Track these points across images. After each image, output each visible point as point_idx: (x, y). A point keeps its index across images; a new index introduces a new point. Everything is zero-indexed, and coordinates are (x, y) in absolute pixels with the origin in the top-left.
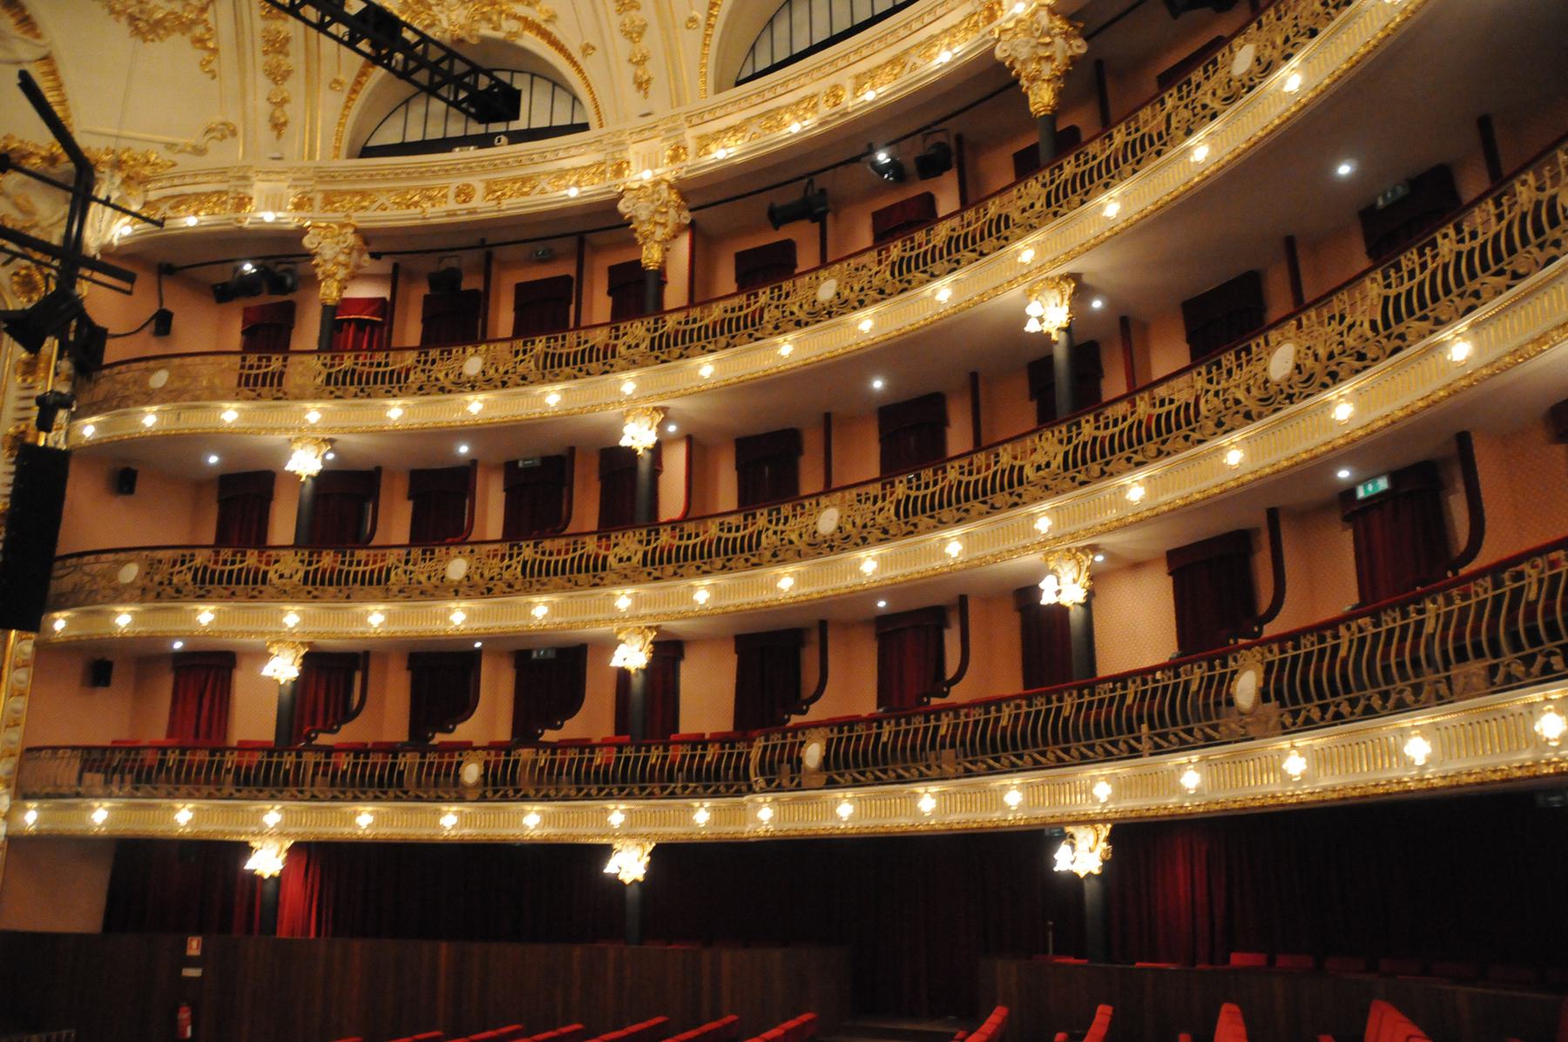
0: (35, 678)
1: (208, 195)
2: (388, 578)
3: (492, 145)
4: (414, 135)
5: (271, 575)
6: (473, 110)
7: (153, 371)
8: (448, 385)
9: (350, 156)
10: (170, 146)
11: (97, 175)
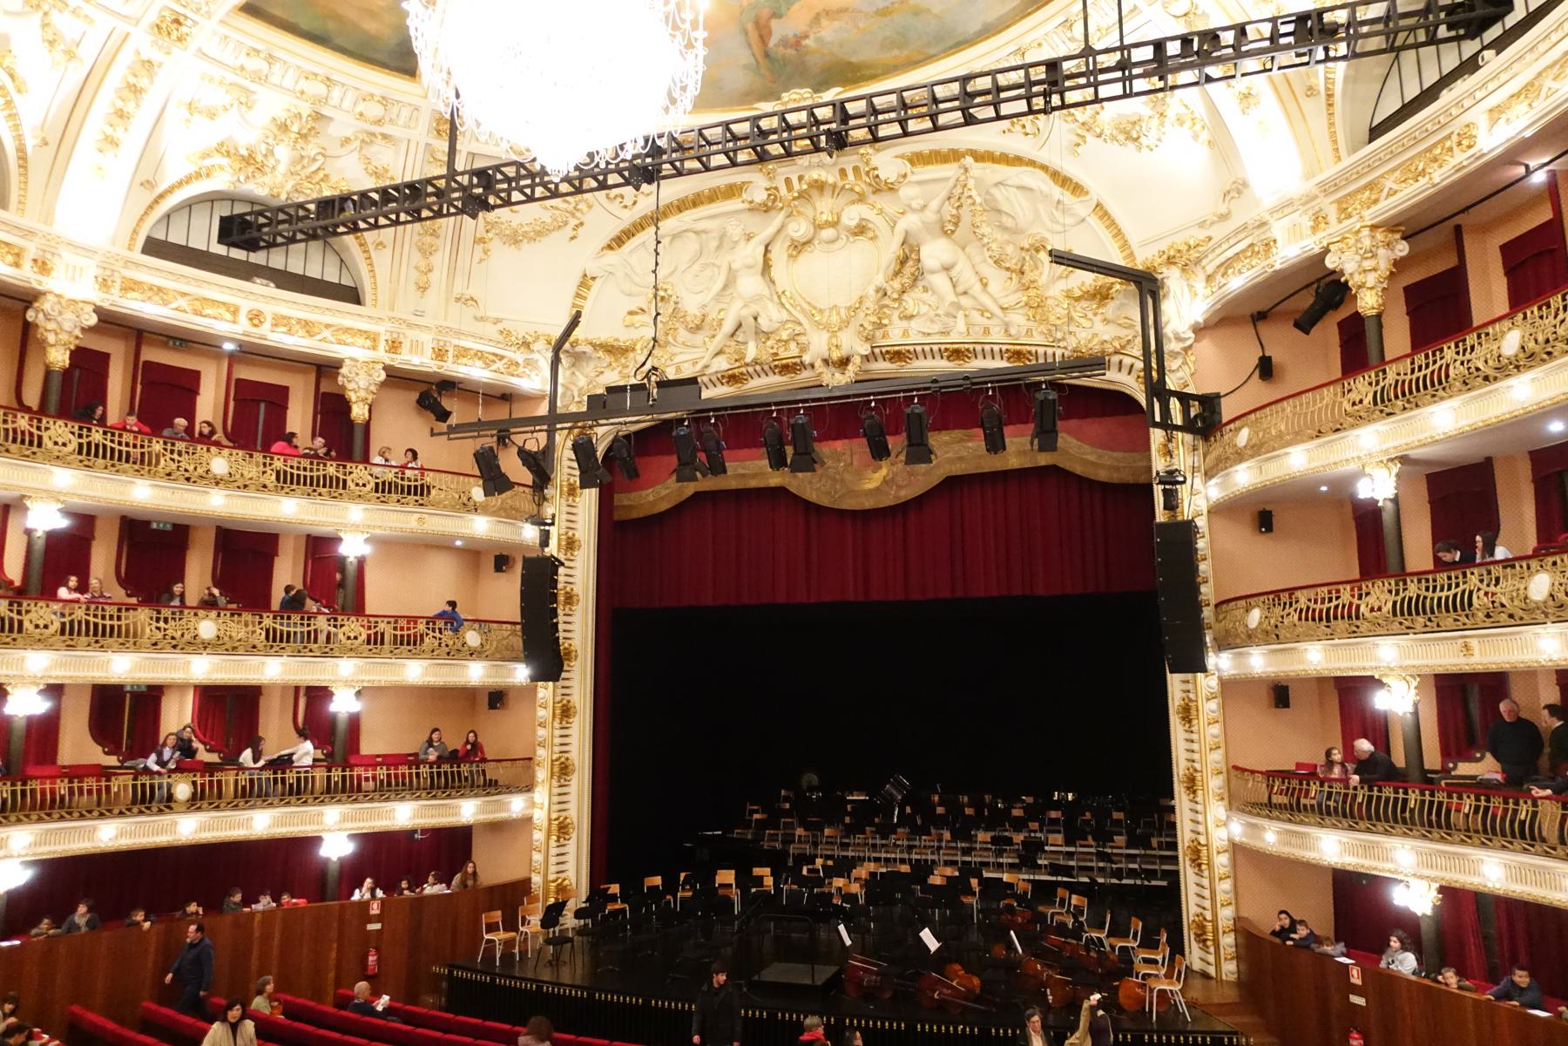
0: (1224, 706)
1: (1244, 251)
2: (1470, 604)
3: (1478, 67)
4: (1412, 91)
5: (1362, 609)
6: (1462, 32)
7: (1238, 429)
8: (1492, 373)
9: (1355, 150)
10: (1202, 225)
11: (1159, 277)
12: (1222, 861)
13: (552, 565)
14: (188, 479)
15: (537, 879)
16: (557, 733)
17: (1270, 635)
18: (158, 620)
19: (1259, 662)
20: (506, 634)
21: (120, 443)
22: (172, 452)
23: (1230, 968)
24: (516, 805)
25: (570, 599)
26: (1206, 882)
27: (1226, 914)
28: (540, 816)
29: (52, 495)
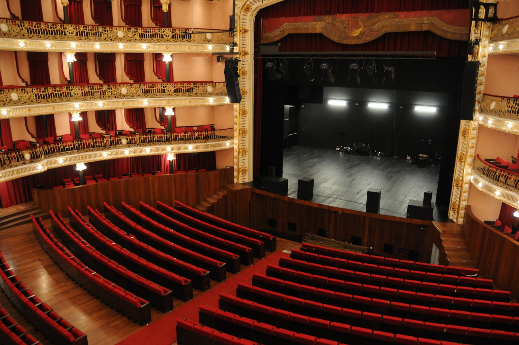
0: (479, 133)
12: (466, 187)
13: (236, 61)
14: (111, 40)
15: (236, 167)
16: (241, 120)
17: (497, 113)
18: (109, 89)
19: (491, 122)
20: (221, 86)
21: (89, 30)
22: (105, 31)
23: (461, 221)
24: (228, 144)
25: (244, 73)
26: (459, 192)
27: (464, 204)
28: (236, 147)
29: (71, 51)
